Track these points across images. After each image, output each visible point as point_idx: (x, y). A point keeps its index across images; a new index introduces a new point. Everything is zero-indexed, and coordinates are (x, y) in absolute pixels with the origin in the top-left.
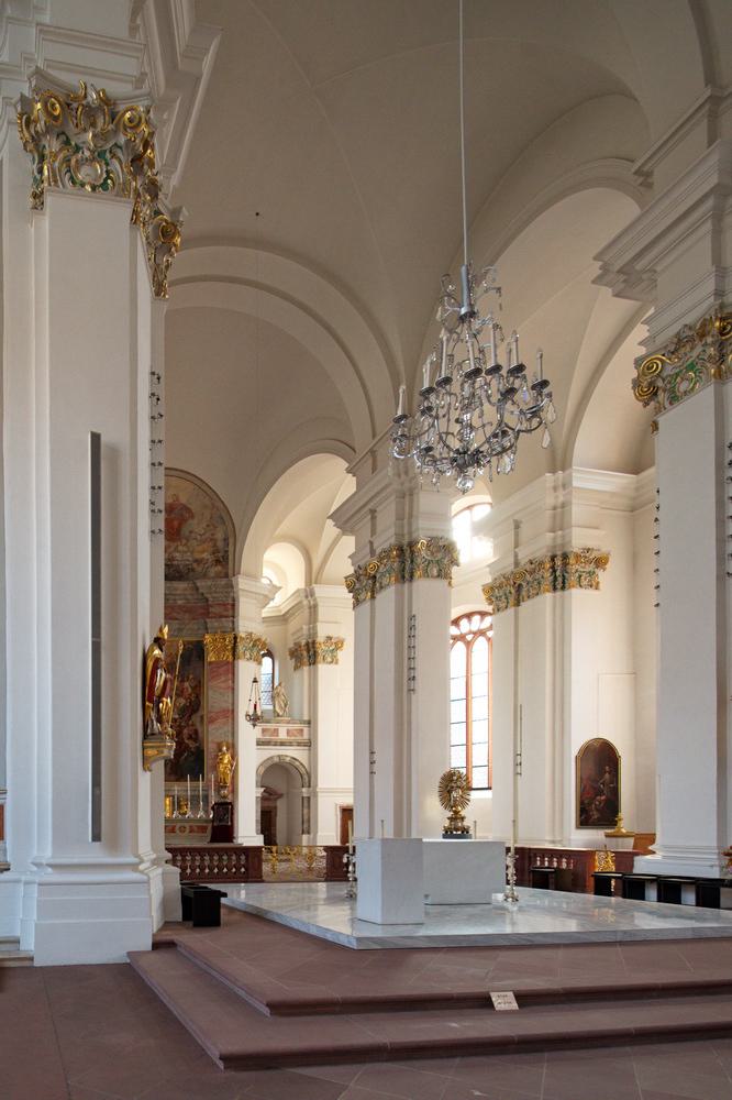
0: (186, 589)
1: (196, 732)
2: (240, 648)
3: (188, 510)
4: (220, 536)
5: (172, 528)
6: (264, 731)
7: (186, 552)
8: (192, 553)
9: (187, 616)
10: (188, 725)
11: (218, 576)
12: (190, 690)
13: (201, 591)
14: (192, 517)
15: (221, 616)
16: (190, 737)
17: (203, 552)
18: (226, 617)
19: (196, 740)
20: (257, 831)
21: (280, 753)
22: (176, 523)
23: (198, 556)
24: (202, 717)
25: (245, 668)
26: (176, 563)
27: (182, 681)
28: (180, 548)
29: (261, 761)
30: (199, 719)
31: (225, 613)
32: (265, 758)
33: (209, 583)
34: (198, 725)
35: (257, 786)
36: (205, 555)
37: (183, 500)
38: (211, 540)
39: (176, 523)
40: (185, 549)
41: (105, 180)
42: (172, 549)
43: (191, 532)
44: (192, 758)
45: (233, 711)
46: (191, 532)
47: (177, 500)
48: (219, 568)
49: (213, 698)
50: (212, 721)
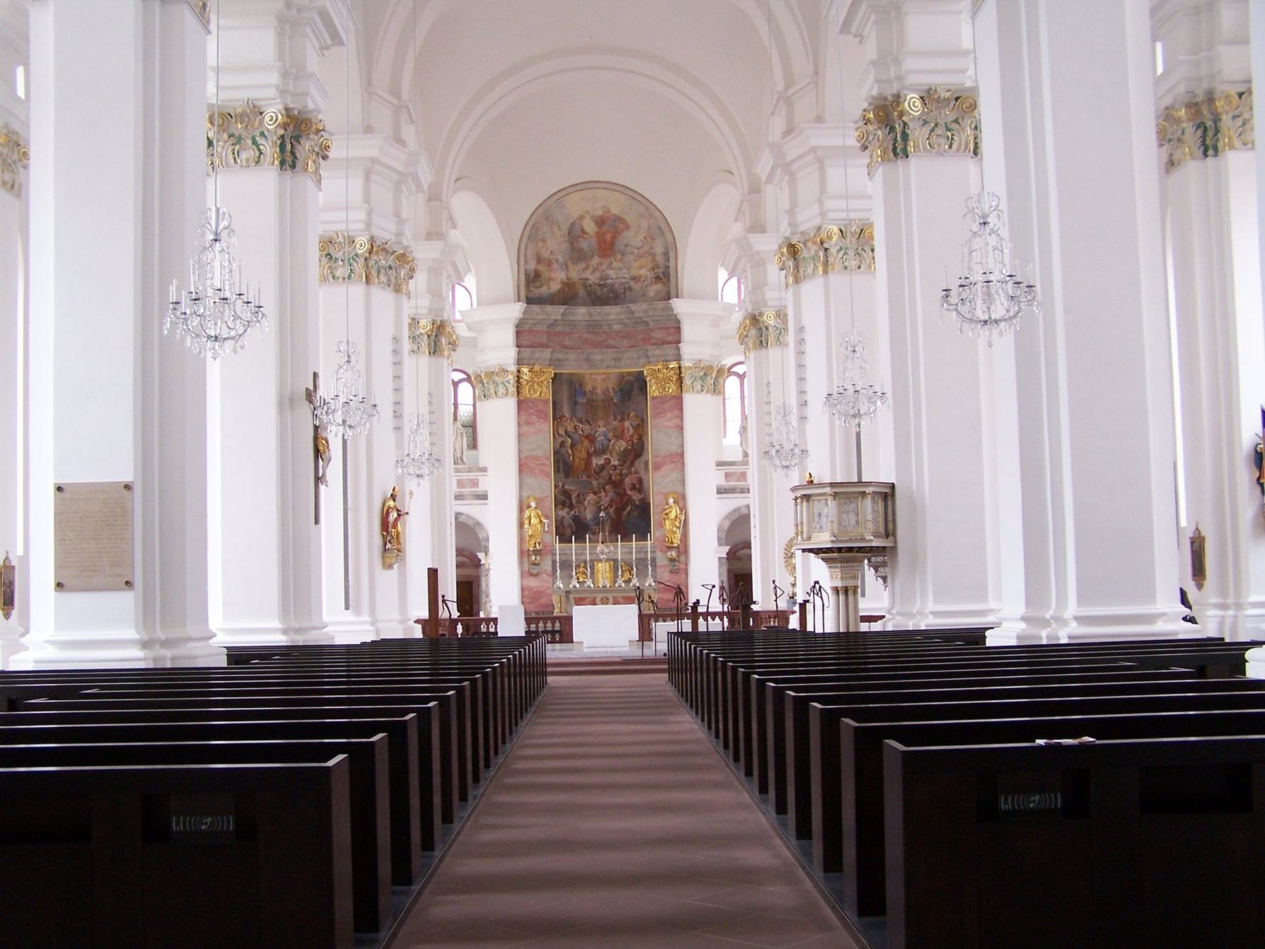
0: (619, 314)
1: (640, 481)
2: (687, 381)
4: (659, 249)
5: (605, 242)
6: (727, 475)
7: (621, 269)
8: (629, 269)
9: (625, 342)
10: (631, 472)
12: (631, 431)
13: (636, 315)
14: (628, 228)
16: (633, 488)
17: (641, 268)
18: (669, 343)
22: (608, 236)
23: (635, 272)
24: (647, 462)
25: (695, 404)
26: (608, 282)
27: (622, 420)
28: (615, 264)
30: (643, 465)
31: (671, 338)
32: (734, 508)
33: (645, 306)
35: (720, 544)
36: (643, 272)
37: (615, 211)
38: (650, 255)
40: (620, 265)
41: (350, 274)
42: (605, 266)
43: (627, 246)
44: (636, 514)
45: (682, 455)
46: (627, 246)
47: (609, 211)
48: (659, 287)
49: (657, 440)
50: (657, 467)
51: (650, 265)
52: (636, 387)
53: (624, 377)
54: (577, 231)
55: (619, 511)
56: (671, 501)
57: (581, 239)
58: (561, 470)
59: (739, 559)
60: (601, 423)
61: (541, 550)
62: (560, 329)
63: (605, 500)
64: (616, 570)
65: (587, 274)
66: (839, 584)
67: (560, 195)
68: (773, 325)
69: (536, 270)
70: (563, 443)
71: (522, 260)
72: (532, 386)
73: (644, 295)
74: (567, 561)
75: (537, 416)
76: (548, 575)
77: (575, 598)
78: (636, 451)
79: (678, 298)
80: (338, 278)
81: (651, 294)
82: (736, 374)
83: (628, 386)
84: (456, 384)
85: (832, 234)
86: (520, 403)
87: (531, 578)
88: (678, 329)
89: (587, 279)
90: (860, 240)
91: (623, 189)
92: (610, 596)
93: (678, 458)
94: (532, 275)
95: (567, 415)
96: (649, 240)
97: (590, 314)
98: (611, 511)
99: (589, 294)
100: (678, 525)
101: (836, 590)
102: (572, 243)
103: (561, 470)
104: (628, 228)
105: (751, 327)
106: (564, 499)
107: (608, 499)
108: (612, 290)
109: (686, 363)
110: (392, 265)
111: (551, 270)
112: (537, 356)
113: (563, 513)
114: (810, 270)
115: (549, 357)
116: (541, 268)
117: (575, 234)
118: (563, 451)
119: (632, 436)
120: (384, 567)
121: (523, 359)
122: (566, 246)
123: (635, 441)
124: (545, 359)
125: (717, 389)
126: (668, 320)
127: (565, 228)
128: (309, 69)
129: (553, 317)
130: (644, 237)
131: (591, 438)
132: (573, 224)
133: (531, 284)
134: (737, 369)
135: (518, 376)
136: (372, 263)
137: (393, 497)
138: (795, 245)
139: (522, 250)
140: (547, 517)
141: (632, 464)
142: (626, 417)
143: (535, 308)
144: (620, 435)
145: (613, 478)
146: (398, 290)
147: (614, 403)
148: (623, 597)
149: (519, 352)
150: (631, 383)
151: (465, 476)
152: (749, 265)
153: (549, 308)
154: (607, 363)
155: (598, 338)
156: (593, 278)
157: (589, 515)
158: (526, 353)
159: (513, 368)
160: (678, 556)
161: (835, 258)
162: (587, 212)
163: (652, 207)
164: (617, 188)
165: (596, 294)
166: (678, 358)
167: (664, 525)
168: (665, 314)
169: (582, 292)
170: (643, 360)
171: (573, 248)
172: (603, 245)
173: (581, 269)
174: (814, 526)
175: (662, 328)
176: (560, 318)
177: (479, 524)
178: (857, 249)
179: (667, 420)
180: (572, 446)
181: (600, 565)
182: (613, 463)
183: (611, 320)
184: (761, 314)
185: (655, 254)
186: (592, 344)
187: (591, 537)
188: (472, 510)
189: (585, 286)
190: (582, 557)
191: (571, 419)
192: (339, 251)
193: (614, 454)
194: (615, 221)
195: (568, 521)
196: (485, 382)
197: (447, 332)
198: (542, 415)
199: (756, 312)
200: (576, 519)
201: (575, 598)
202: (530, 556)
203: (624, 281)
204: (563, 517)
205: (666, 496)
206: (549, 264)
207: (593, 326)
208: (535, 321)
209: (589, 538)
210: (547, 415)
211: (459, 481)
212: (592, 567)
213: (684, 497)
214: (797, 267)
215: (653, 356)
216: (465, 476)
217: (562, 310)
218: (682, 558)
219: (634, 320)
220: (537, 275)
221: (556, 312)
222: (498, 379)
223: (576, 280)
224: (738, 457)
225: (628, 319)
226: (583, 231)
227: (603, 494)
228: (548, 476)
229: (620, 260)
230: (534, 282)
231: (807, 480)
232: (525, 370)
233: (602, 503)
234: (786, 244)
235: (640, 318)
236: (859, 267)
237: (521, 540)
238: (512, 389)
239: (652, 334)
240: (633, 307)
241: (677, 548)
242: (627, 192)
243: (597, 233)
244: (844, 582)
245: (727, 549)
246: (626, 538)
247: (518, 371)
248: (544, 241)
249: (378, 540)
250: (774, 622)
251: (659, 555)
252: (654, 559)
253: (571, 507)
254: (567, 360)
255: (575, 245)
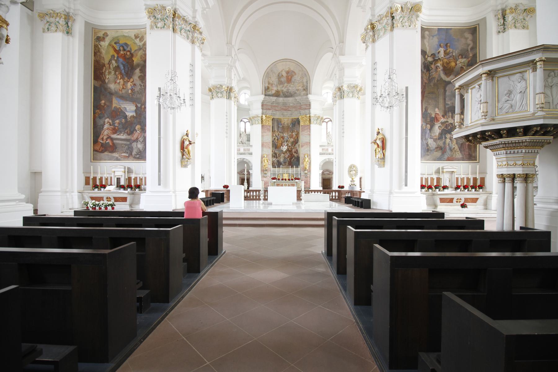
1: (297, 150)
2: (312, 120)
3: (293, 72)
4: (305, 80)
5: (289, 79)
6: (323, 149)
9: (294, 109)
10: (294, 148)
11: (304, 95)
12: (295, 135)
13: (297, 100)
14: (295, 74)
15: (306, 109)
16: (295, 152)
17: (299, 87)
18: (307, 109)
19: (297, 153)
20: (320, 186)
21: (328, 157)
22: (290, 77)
23: (297, 88)
24: (299, 145)
25: (314, 127)
26: (289, 91)
27: (292, 132)
28: (291, 86)
29: (321, 161)
30: (298, 146)
31: (307, 108)
33: (300, 97)
34: (298, 148)
36: (300, 88)
37: (292, 69)
38: (302, 83)
39: (290, 77)
40: (293, 86)
43: (295, 80)
44: (295, 160)
45: (310, 143)
46: (295, 80)
47: (290, 69)
48: (304, 92)
49: (303, 139)
50: (302, 146)
51: (302, 86)
52: (297, 122)
53: (293, 120)
54: (280, 75)
55: (290, 159)
56: (306, 156)
57: (282, 78)
58: (274, 147)
59: (324, 174)
60: (286, 133)
61: (267, 170)
62: (274, 105)
63: (287, 156)
64: (289, 176)
65: (283, 89)
66: (505, 171)
67: (275, 63)
68: (346, 90)
69: (268, 87)
70: (275, 138)
71: (264, 83)
72: (266, 121)
73: (300, 95)
74: (275, 173)
75: (268, 130)
76: (269, 177)
77: (276, 184)
78: (296, 142)
79: (310, 94)
80: (159, 28)
81: (302, 94)
82: (325, 122)
83: (294, 122)
84: (245, 123)
85: (398, 8)
86: (262, 126)
87: (264, 178)
88: (310, 105)
89: (283, 90)
90: (411, 13)
91: (294, 62)
92: (287, 184)
93: (309, 144)
94: (267, 88)
95: (276, 131)
96: (302, 78)
97: (284, 100)
98: (288, 159)
99: (283, 94)
100: (308, 163)
101: (503, 178)
102: (279, 79)
103: (274, 147)
104: (295, 74)
105: (338, 92)
106: (275, 155)
107: (287, 155)
108: (290, 94)
109: (312, 115)
110: (190, 30)
111: (272, 87)
112: (267, 112)
113: (274, 159)
114: (381, 34)
115: (271, 113)
116: (269, 86)
117: (280, 76)
118: (275, 141)
119: (295, 137)
120: (182, 167)
121: (263, 113)
122: (277, 80)
123: (296, 139)
124: (270, 113)
125: (320, 124)
126: (307, 102)
127: (277, 74)
128: (232, 78)
129: (273, 101)
130: (301, 77)
131: (283, 138)
132: (279, 73)
133: (266, 91)
134: (325, 120)
135: (262, 118)
136: (177, 22)
137: (187, 135)
138: (374, 24)
139: (264, 80)
140: (269, 160)
141: (295, 145)
142: (293, 131)
143: (267, 97)
144: (291, 137)
145: (289, 149)
146: (193, 42)
147: (290, 128)
148: (291, 184)
149: (262, 111)
150: (296, 121)
151: (246, 148)
152: (338, 70)
153: (271, 97)
154: (288, 115)
155: (286, 108)
156: (285, 90)
157: (282, 160)
158: (265, 111)
159: (260, 115)
160: (308, 173)
161: (399, 21)
162: (283, 69)
163: (302, 67)
164: (293, 61)
165: (286, 95)
166: (310, 113)
167: (304, 163)
168: (306, 100)
169: (281, 94)
170: (299, 115)
171: (279, 80)
172: (288, 80)
173: (281, 87)
174: (500, 106)
175: (305, 105)
176: (275, 101)
177: (249, 162)
178: (409, 17)
179: (306, 132)
180: (277, 140)
181: (285, 175)
182: (289, 145)
183: (290, 102)
184: (342, 87)
185: (303, 82)
186: (284, 110)
187: (282, 166)
188: (247, 157)
189: (282, 92)
190: (279, 172)
191: (277, 132)
192: (159, 14)
193: (290, 143)
194: (292, 72)
195: (276, 162)
196: (252, 120)
197: (233, 91)
198: (268, 130)
199: (340, 86)
200: (278, 161)
201: (276, 184)
202: (264, 171)
203: (294, 91)
204: (274, 160)
205: (305, 155)
206: (272, 85)
207: (284, 104)
208: (267, 102)
209: (282, 167)
210: (270, 130)
211: (244, 149)
212: (282, 175)
213: (310, 155)
214: (374, 35)
215: (302, 113)
216: (246, 148)
217: (275, 98)
218: (309, 173)
219: (296, 102)
220: (268, 88)
221: (274, 99)
222: (256, 119)
223: (280, 90)
224: (326, 144)
225: (295, 102)
226: (282, 76)
227: (286, 154)
228: (270, 148)
229: (293, 85)
230: (267, 90)
231: (377, 131)
232: (264, 116)
233: (286, 156)
234: (370, 23)
235: (298, 101)
236: (410, 26)
237: (262, 167)
238: (260, 122)
239: (302, 107)
240: (297, 98)
241: (307, 170)
242: (296, 63)
243: (286, 76)
244: (525, 169)
245: (322, 171)
246: (292, 167)
247: (262, 116)
248: (270, 78)
249: (178, 154)
250: (348, 195)
251: (302, 172)
252: (300, 174)
253: (277, 158)
254: (276, 114)
255: (280, 79)
